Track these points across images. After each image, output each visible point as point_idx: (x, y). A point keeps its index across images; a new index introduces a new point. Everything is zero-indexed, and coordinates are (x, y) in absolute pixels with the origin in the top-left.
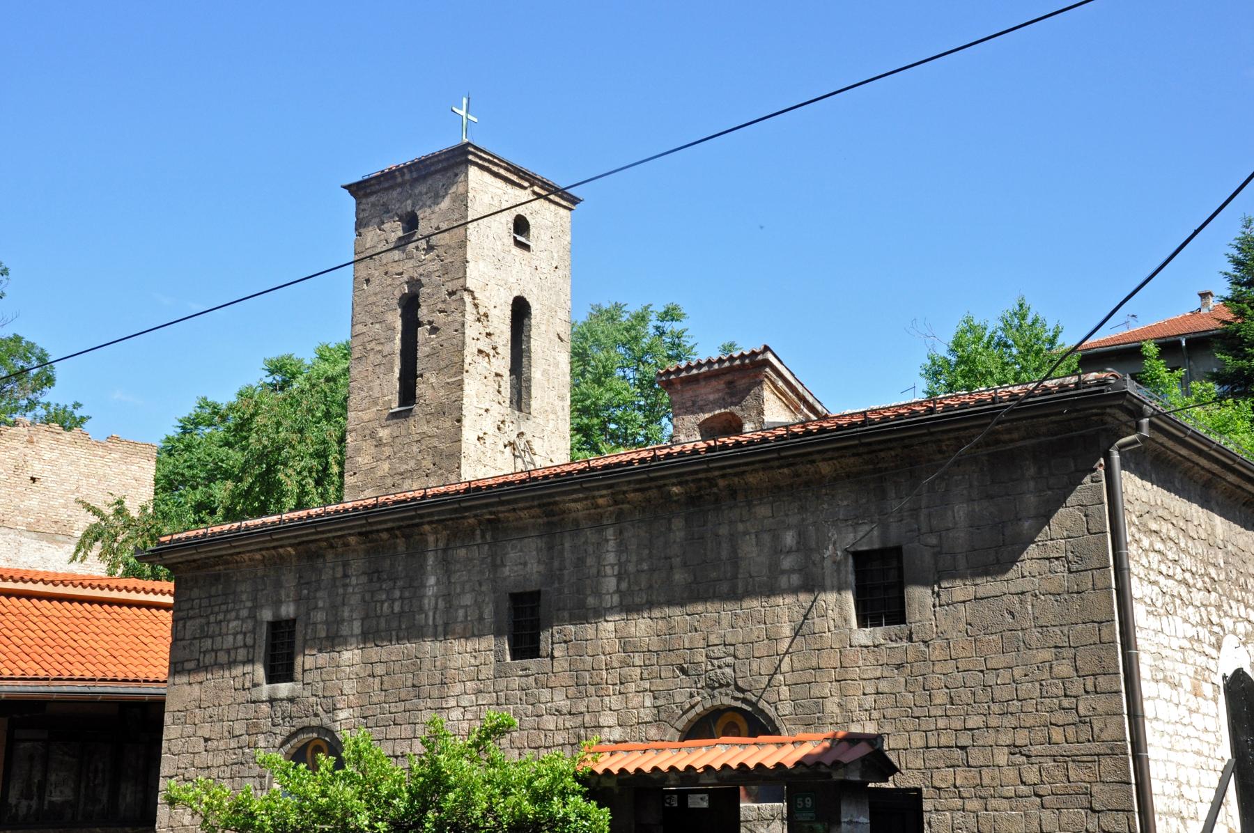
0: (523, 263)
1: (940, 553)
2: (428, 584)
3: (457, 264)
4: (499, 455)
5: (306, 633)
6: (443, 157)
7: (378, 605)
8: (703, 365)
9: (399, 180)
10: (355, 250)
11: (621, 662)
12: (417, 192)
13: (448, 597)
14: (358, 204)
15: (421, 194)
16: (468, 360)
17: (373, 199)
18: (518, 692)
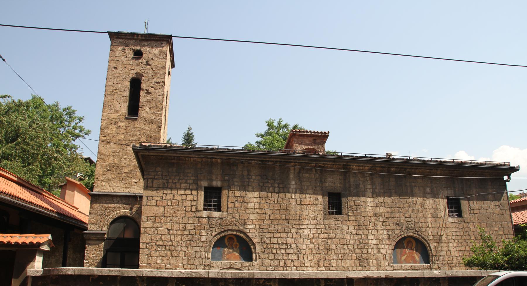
2: (291, 184)
7: (267, 188)
8: (308, 132)
9: (135, 37)
10: (110, 55)
11: (375, 220)
17: (120, 40)
18: (333, 225)
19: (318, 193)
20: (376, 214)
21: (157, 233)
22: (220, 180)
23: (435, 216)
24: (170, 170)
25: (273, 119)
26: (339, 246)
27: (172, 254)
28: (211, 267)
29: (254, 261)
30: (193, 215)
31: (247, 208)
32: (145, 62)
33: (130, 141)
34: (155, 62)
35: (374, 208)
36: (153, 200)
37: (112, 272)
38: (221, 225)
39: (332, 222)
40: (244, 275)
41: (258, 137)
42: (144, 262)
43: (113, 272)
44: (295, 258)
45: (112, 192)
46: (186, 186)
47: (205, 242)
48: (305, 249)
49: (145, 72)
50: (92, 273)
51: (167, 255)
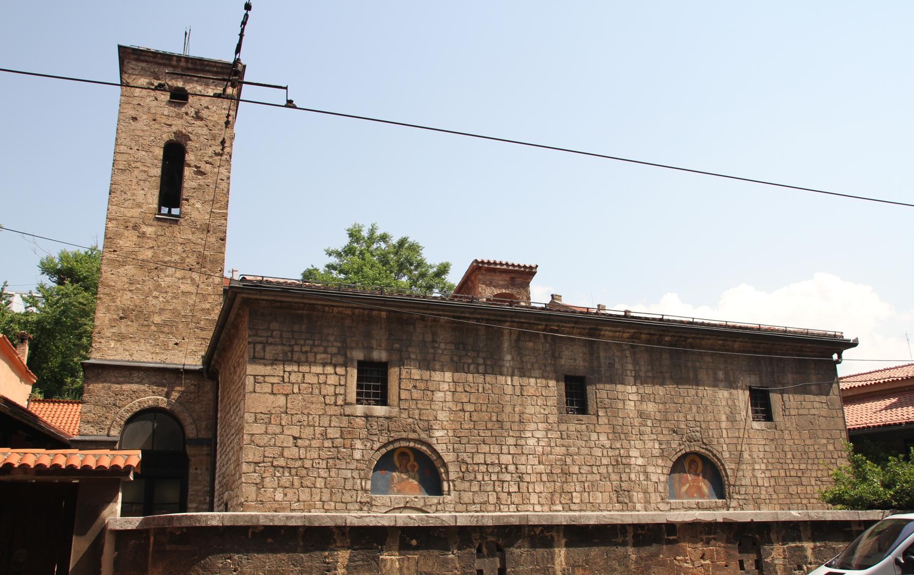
2: (505, 359)
6: (220, 65)
7: (466, 366)
8: (503, 265)
11: (640, 423)
17: (144, 65)
19: (548, 376)
20: (641, 414)
22: (385, 349)
23: (731, 419)
24: (296, 328)
25: (361, 225)
26: (585, 469)
27: (302, 483)
28: (372, 505)
29: (446, 494)
30: (339, 412)
31: (432, 400)
32: (193, 112)
33: (165, 262)
34: (213, 114)
35: (638, 403)
36: (265, 382)
37: (291, 520)
38: (389, 431)
39: (572, 427)
40: (513, 520)
41: (330, 255)
42: (250, 499)
43: (293, 520)
44: (514, 488)
45: (128, 361)
46: (326, 359)
47: (362, 461)
48: (530, 474)
49: (194, 133)
50: (255, 523)
51: (293, 485)
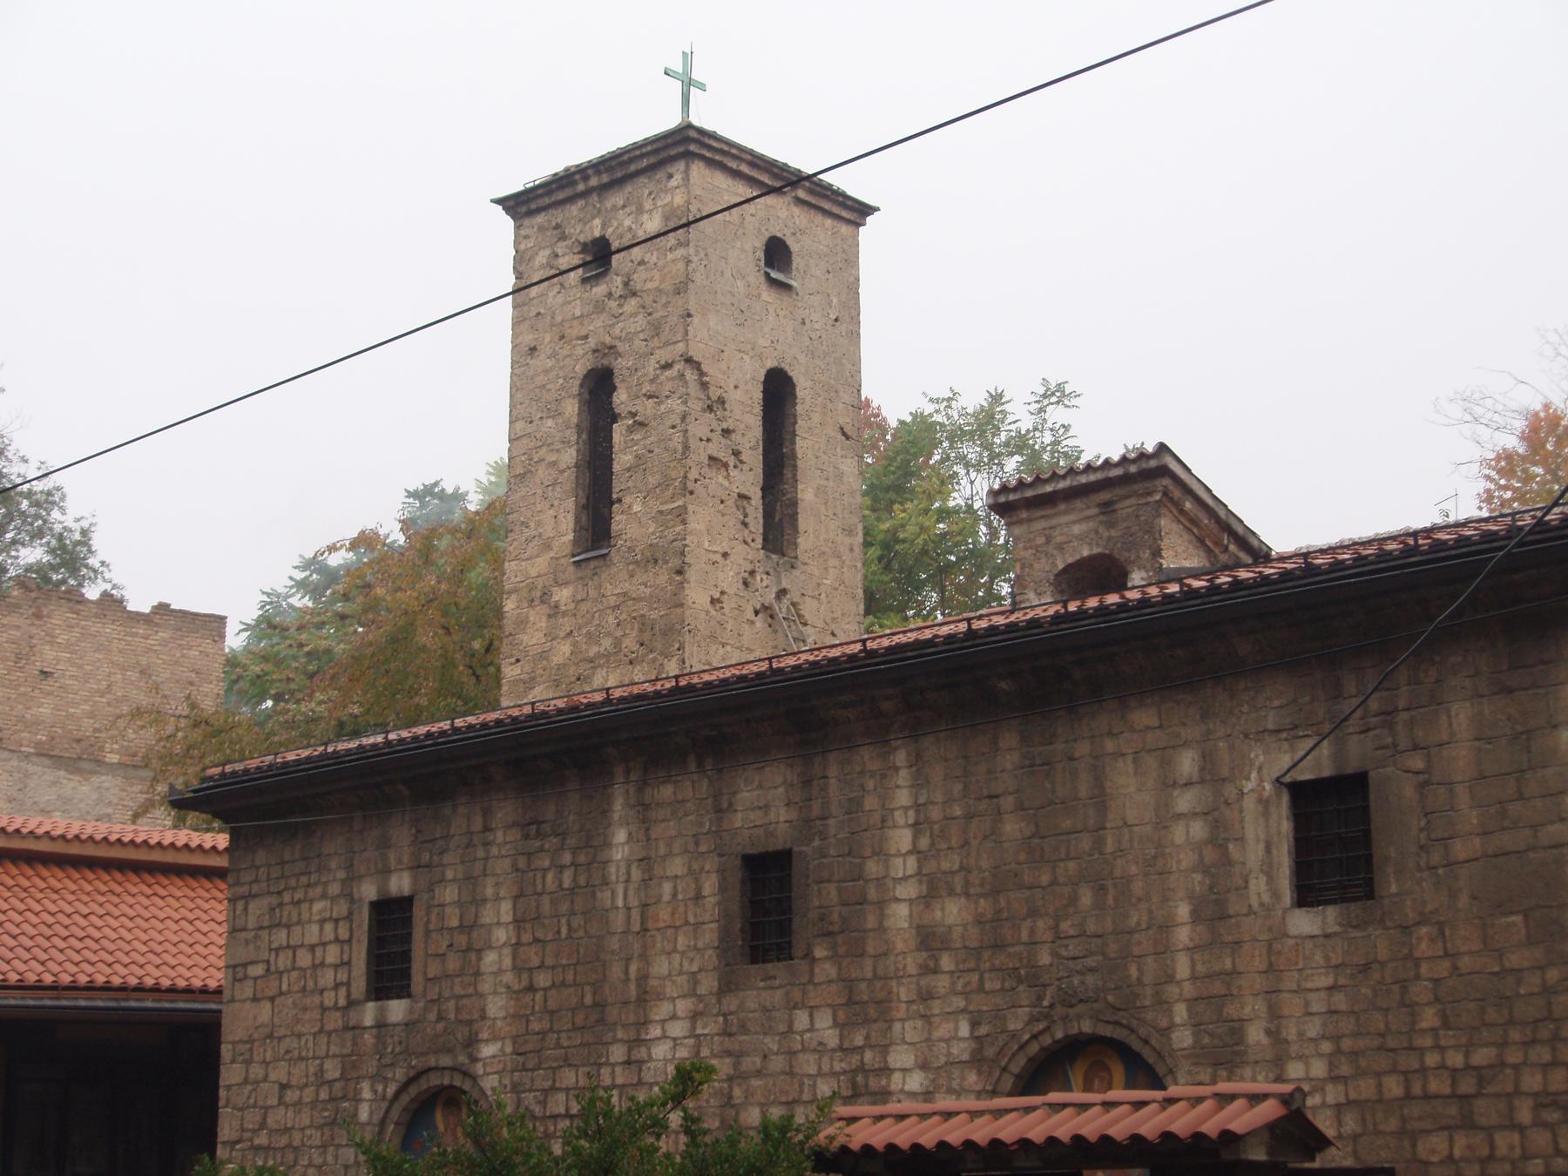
0: (781, 313)
1: (1426, 783)
3: (673, 319)
4: (746, 626)
5: (428, 922)
6: (649, 148)
7: (539, 875)
12: (608, 205)
13: (645, 861)
14: (518, 228)
15: (614, 207)
16: (693, 474)
17: (540, 219)
20: (929, 940)
21: (255, 1106)
